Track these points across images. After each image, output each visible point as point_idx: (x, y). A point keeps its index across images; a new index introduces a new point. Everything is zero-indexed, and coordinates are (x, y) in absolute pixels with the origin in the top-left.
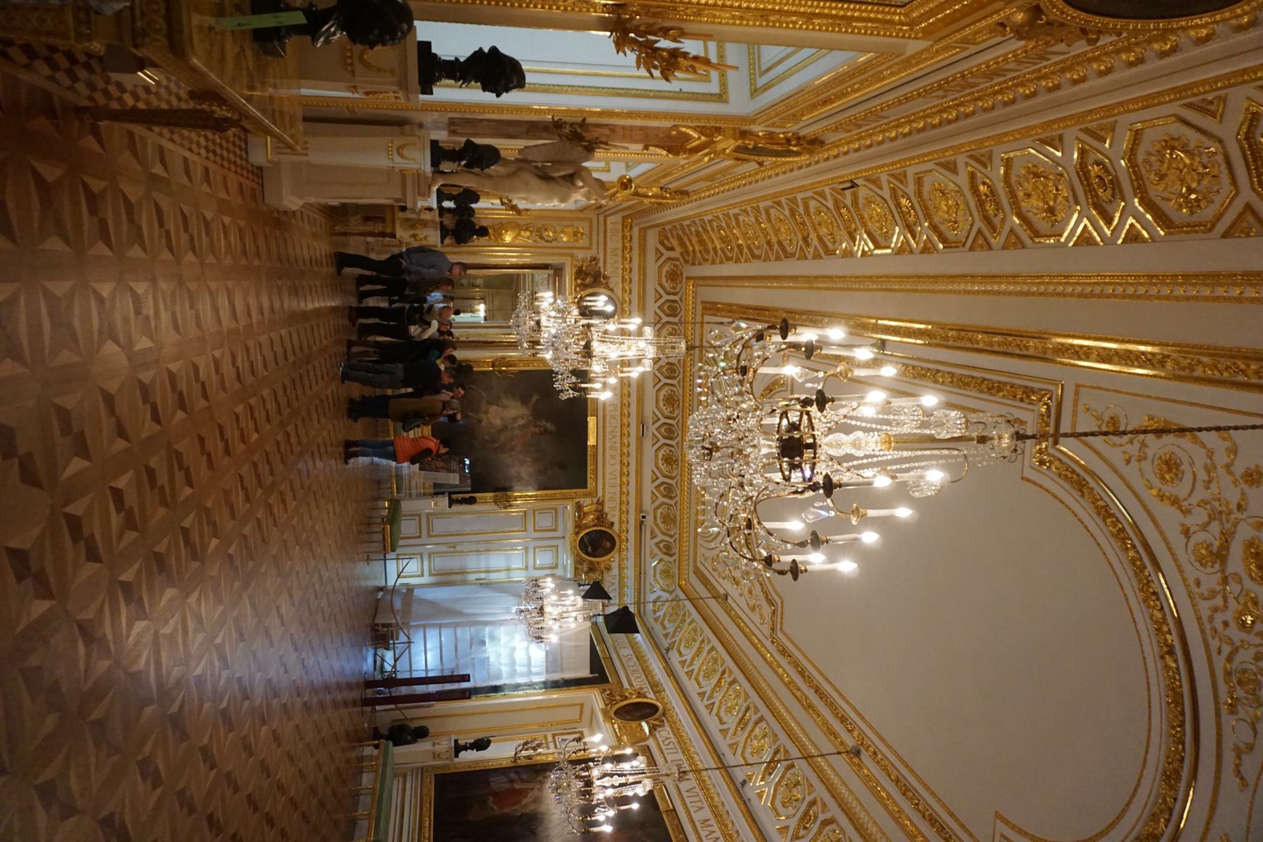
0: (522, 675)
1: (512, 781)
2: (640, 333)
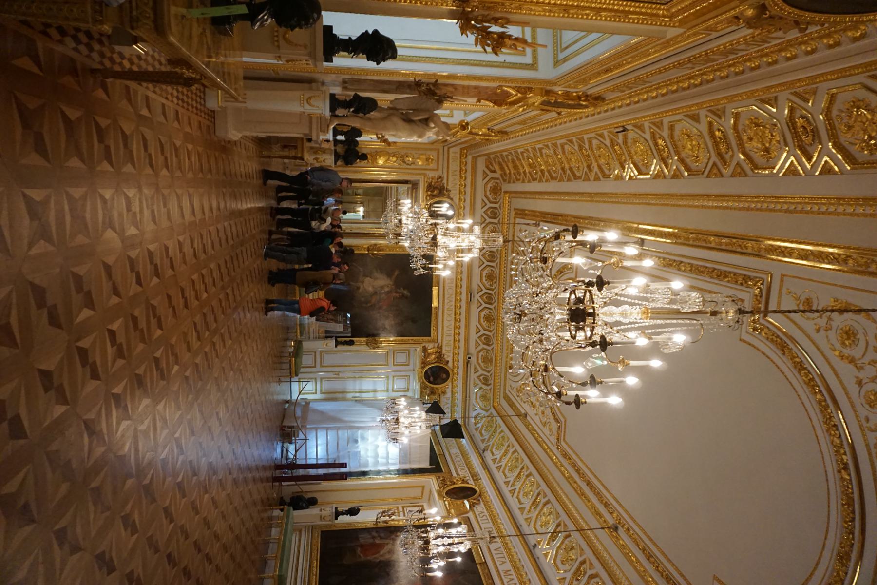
0: (383, 464)
1: (374, 538)
2: (471, 230)
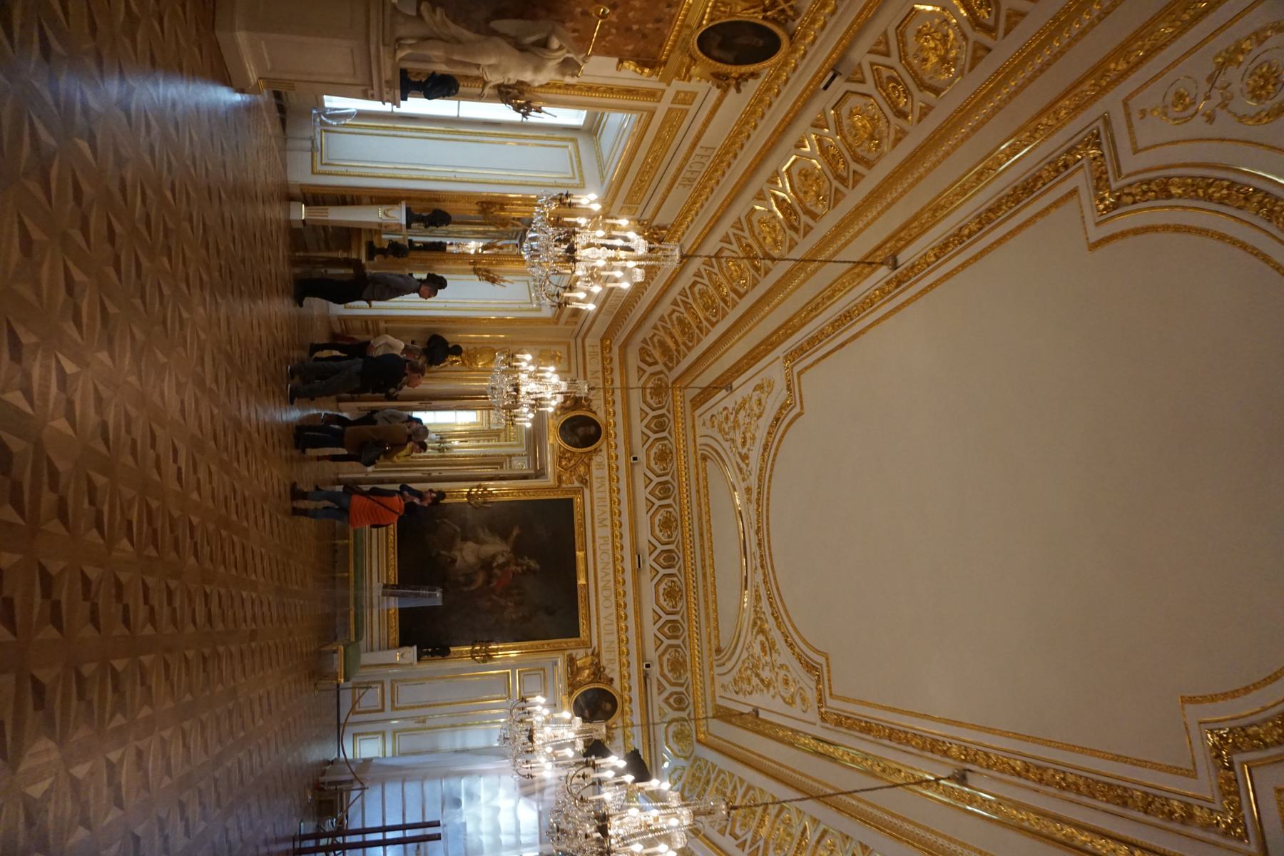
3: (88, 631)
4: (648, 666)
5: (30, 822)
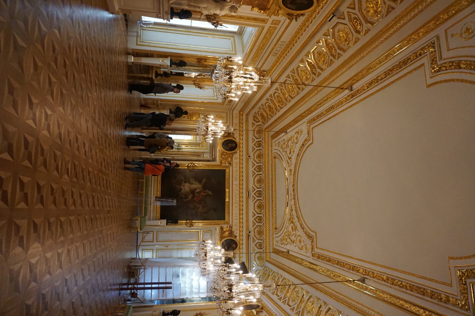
0: (196, 293)
3: (53, 207)
4: (249, 232)
5: (31, 271)
